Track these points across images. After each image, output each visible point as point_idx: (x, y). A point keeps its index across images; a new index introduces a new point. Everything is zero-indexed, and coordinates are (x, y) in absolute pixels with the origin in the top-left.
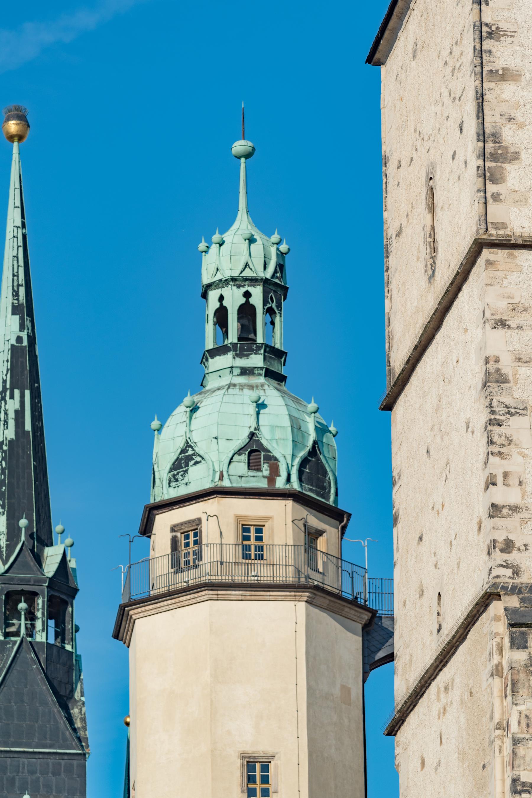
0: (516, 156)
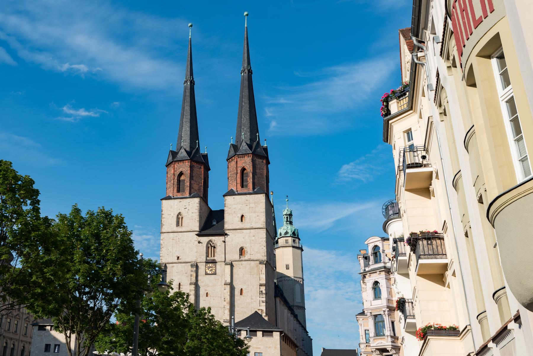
0: (164, 225)
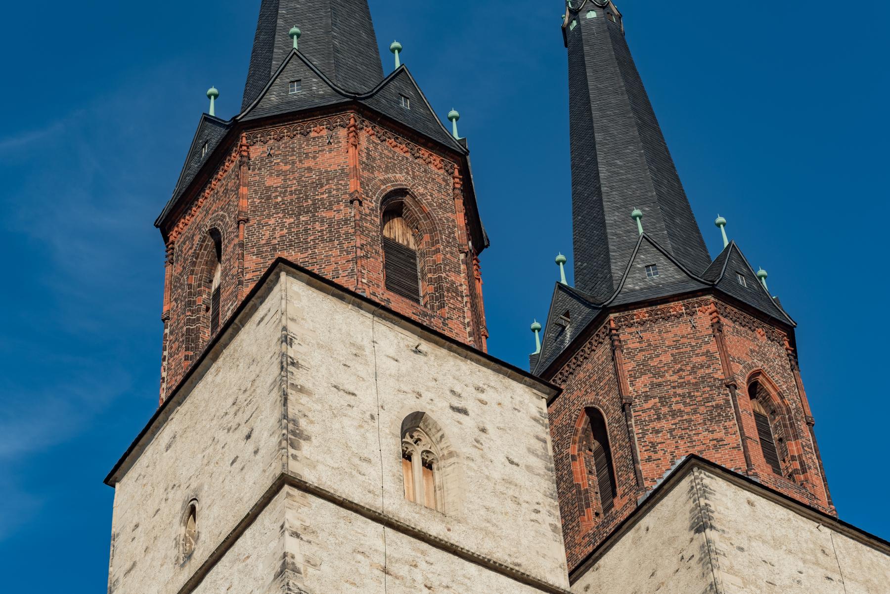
0: (308, 439)
